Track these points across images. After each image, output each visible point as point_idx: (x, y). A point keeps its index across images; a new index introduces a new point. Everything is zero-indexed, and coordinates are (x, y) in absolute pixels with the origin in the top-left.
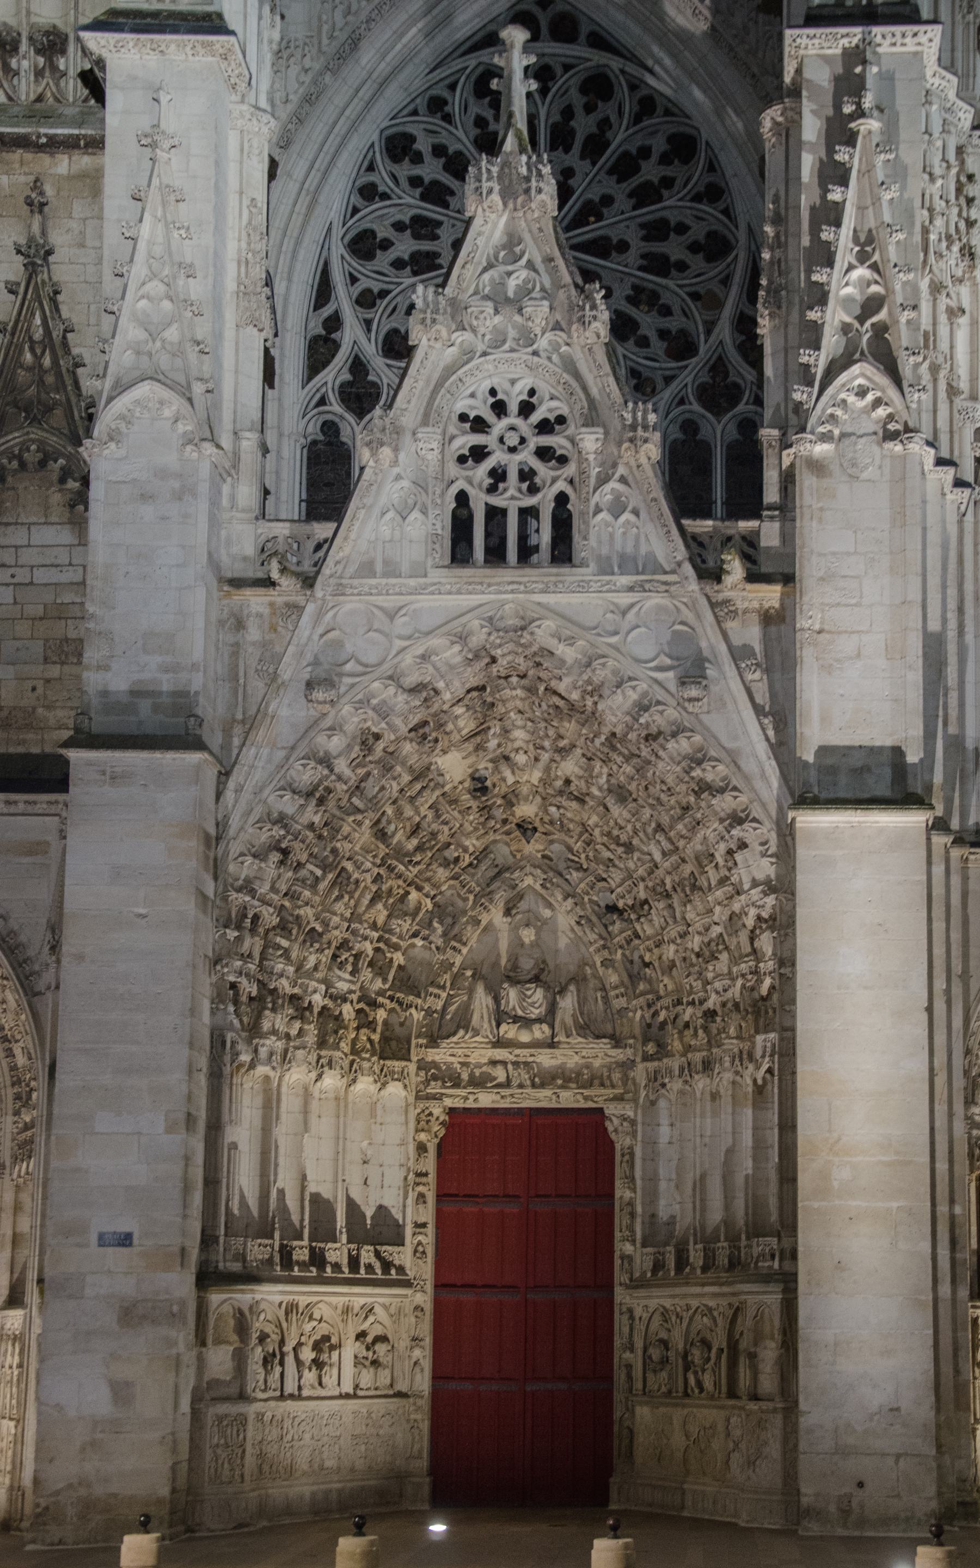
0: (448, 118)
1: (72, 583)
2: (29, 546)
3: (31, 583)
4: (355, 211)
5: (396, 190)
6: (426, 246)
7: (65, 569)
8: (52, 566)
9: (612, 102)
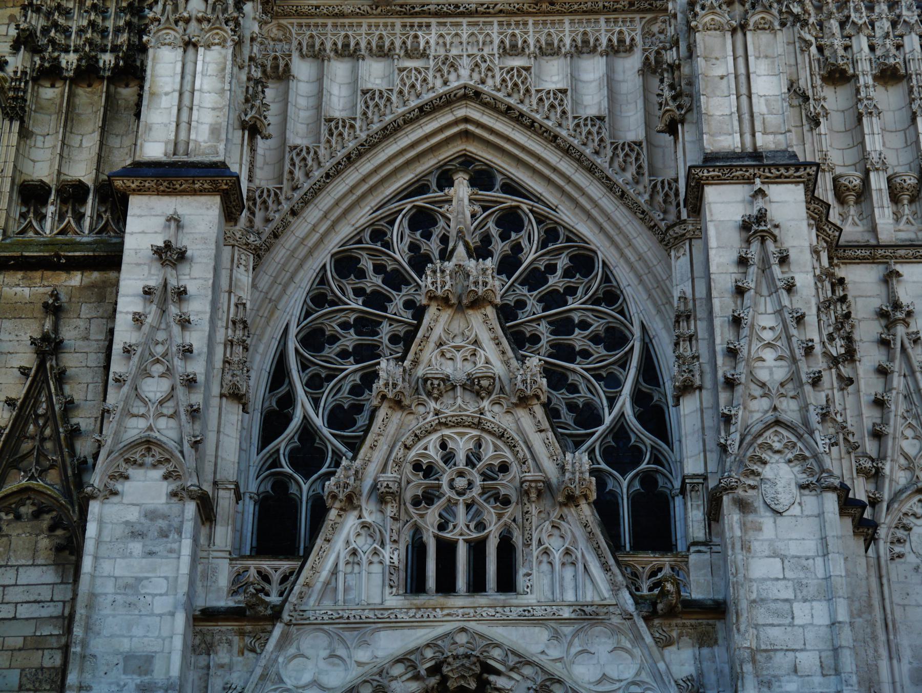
0: (388, 245)
1: (51, 617)
2: (16, 585)
3: (15, 618)
4: (308, 314)
5: (343, 298)
6: (367, 340)
7: (46, 605)
8: (35, 602)
9: (523, 233)
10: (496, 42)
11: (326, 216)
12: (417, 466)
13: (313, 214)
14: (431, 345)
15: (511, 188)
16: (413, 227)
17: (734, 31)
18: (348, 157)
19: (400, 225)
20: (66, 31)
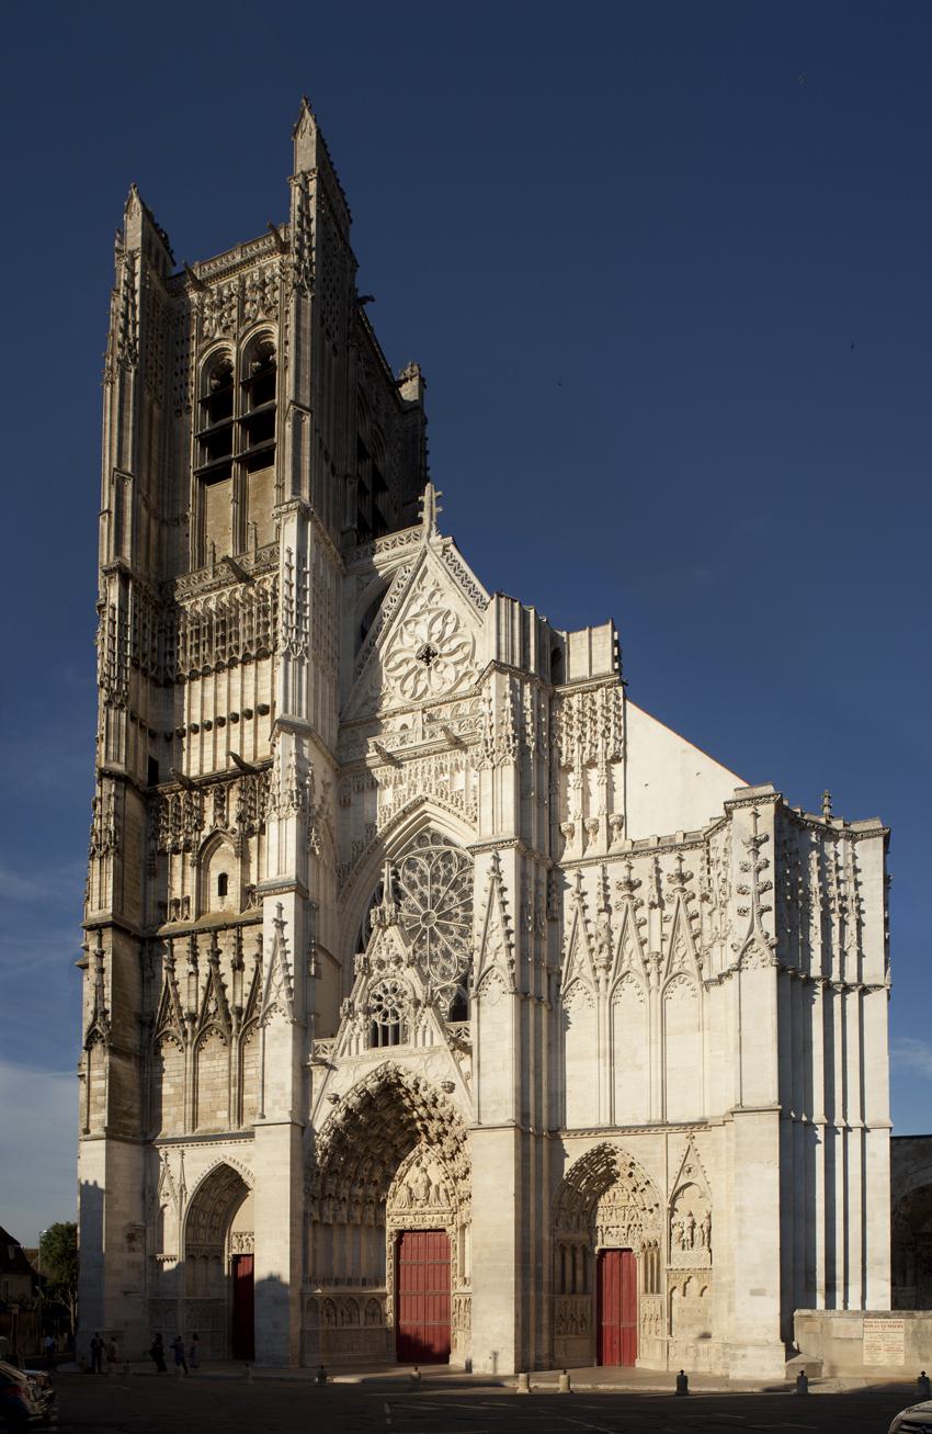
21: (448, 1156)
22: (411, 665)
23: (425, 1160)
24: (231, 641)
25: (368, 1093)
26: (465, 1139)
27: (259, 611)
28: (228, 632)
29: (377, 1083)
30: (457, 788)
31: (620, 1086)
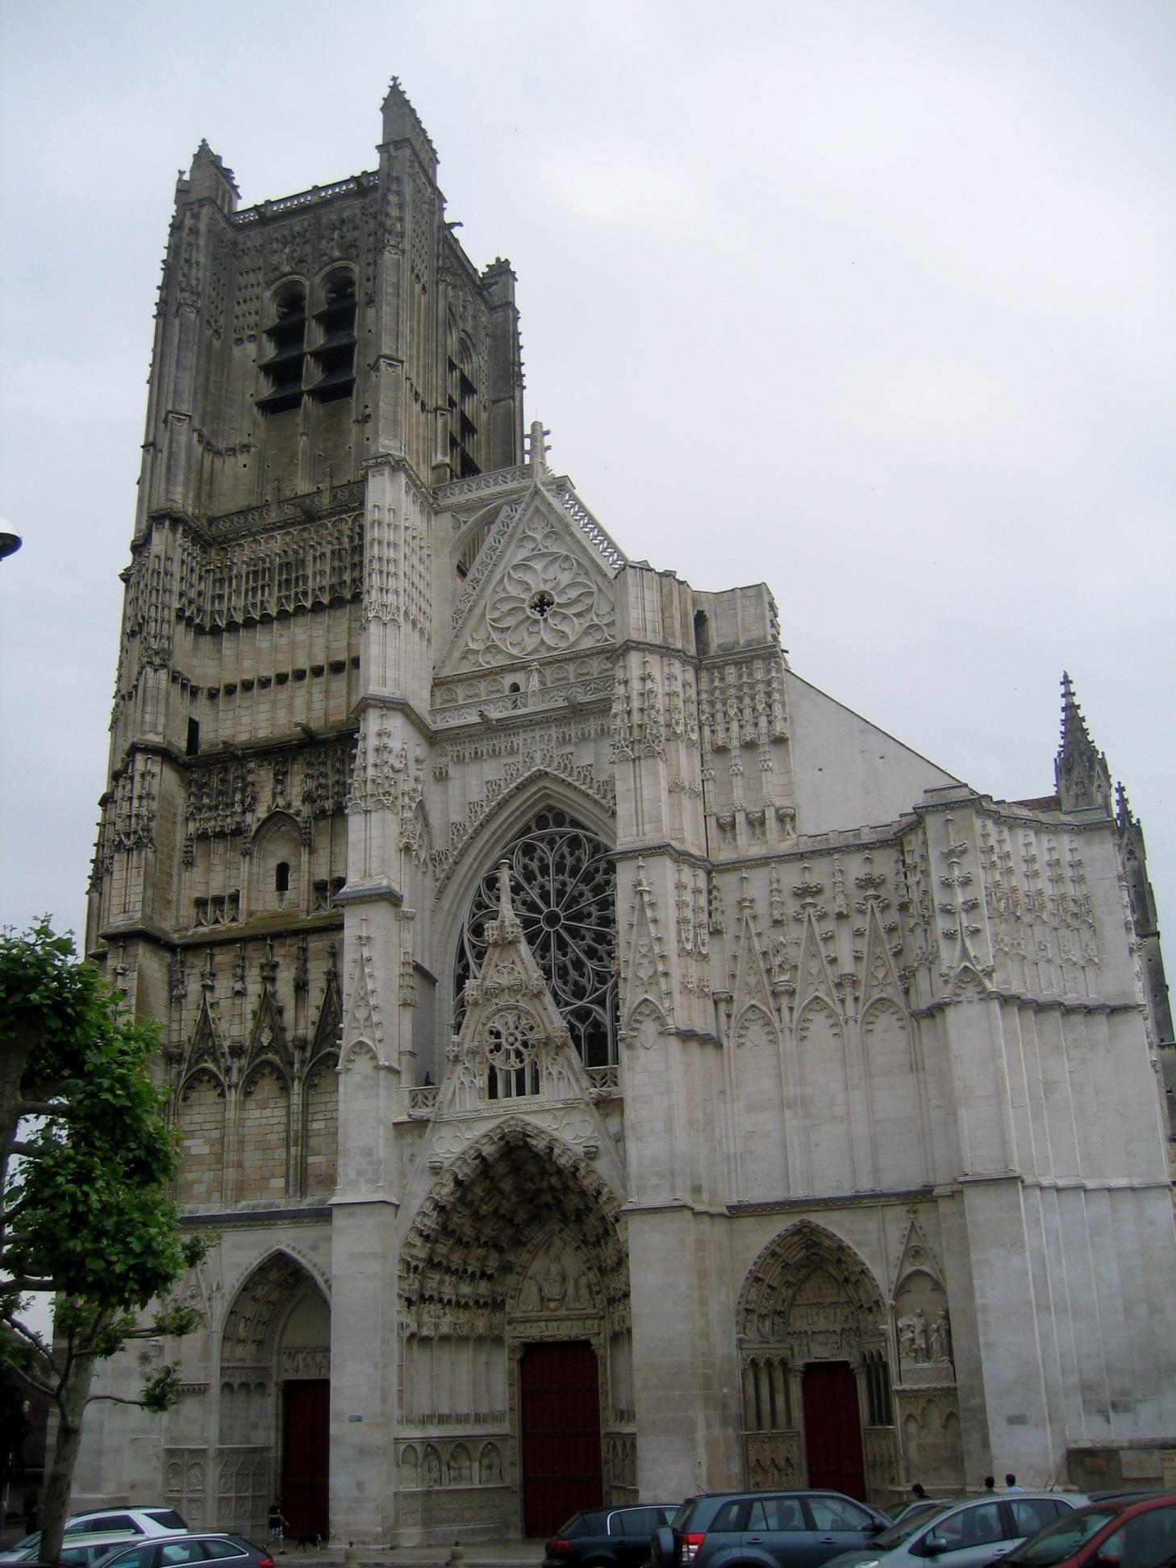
10: (555, 738)
11: (475, 859)
12: (491, 1033)
13: (468, 860)
14: (492, 967)
15: (575, 823)
16: (524, 855)
17: (634, 760)
18: (481, 825)
19: (518, 853)
20: (326, 786)
21: (591, 1239)
22: (521, 617)
23: (557, 1241)
24: (297, 585)
25: (484, 1159)
26: (617, 1220)
27: (333, 552)
28: (294, 575)
29: (493, 1147)
30: (586, 762)
31: (817, 1145)
